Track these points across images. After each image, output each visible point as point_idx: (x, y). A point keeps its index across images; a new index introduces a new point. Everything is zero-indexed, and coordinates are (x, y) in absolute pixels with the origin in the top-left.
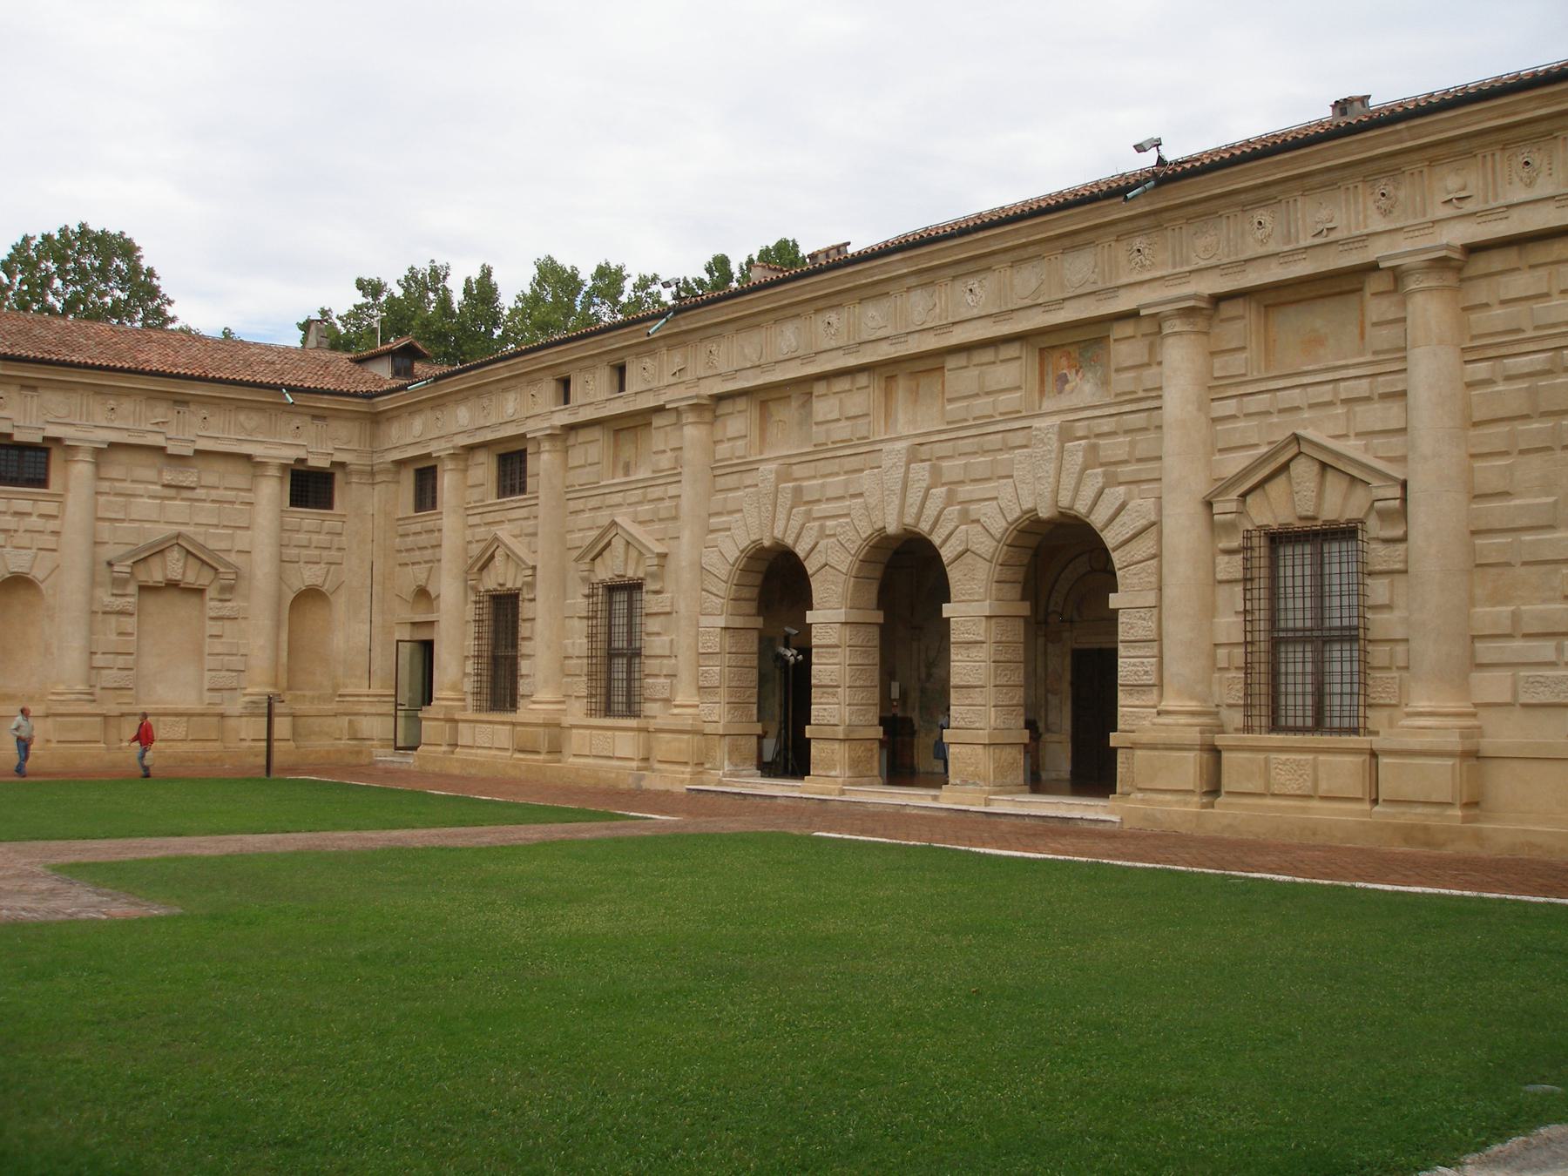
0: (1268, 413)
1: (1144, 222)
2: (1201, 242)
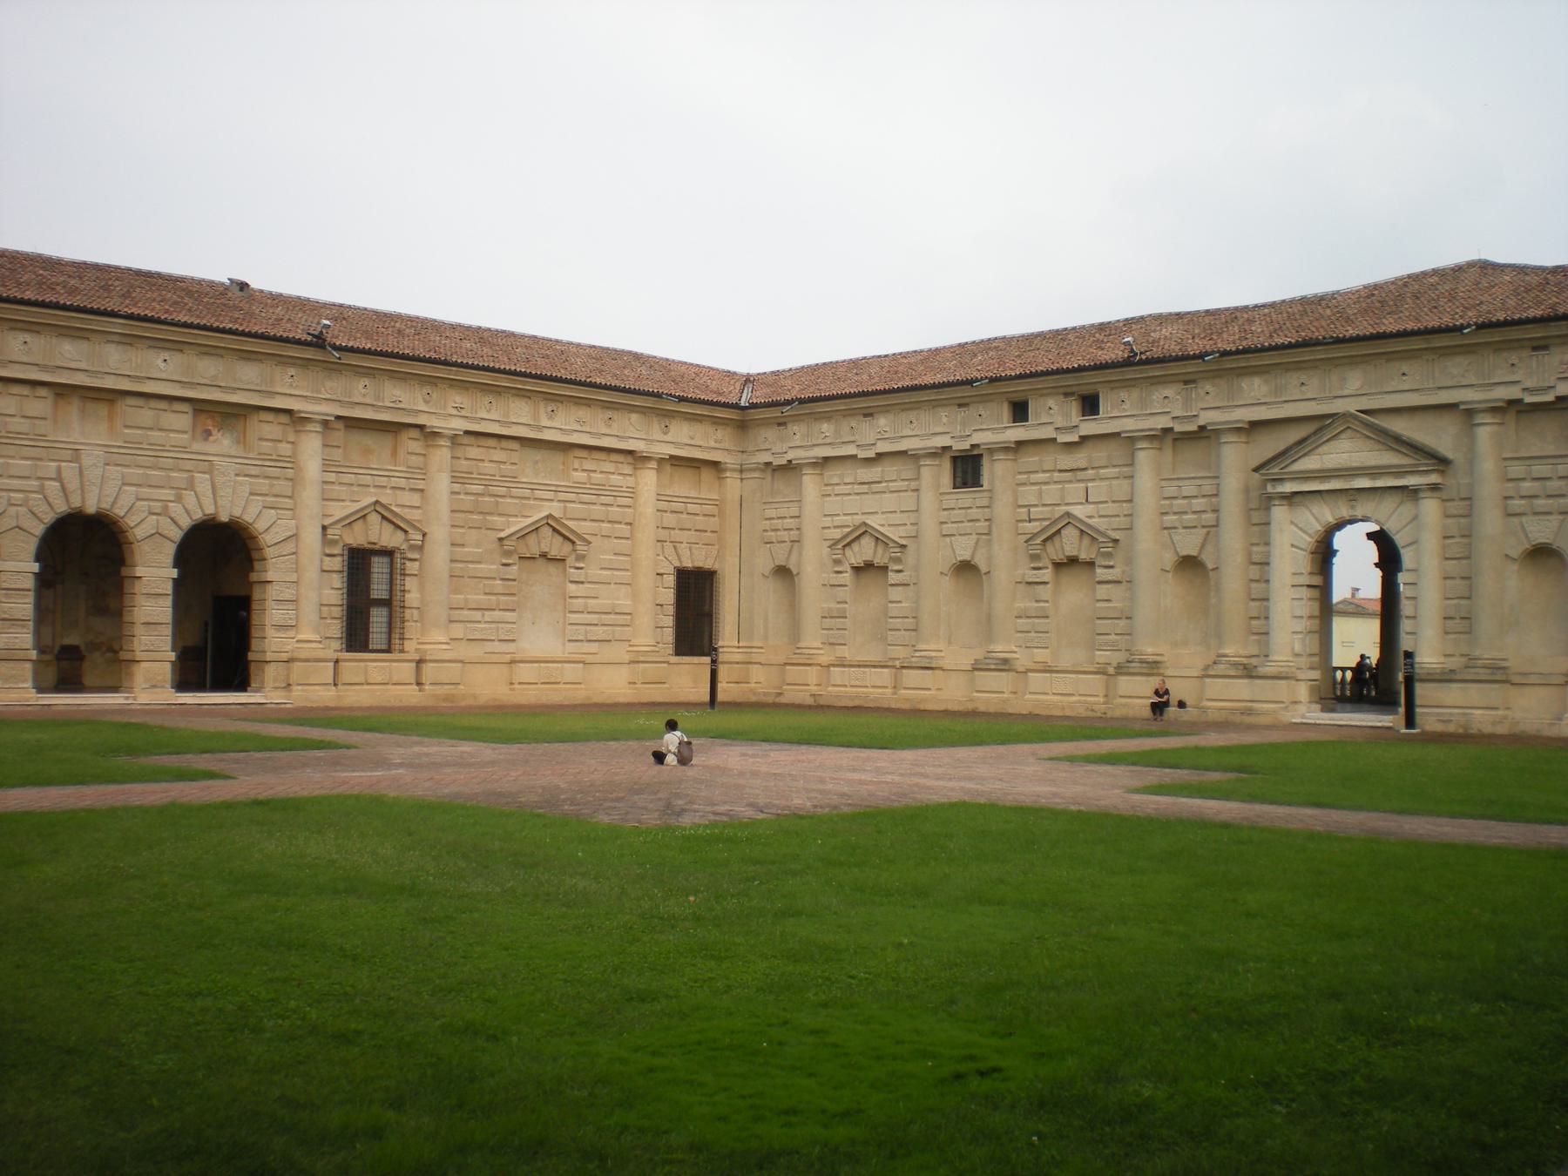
0: (352, 485)
1: (300, 362)
2: (329, 384)
